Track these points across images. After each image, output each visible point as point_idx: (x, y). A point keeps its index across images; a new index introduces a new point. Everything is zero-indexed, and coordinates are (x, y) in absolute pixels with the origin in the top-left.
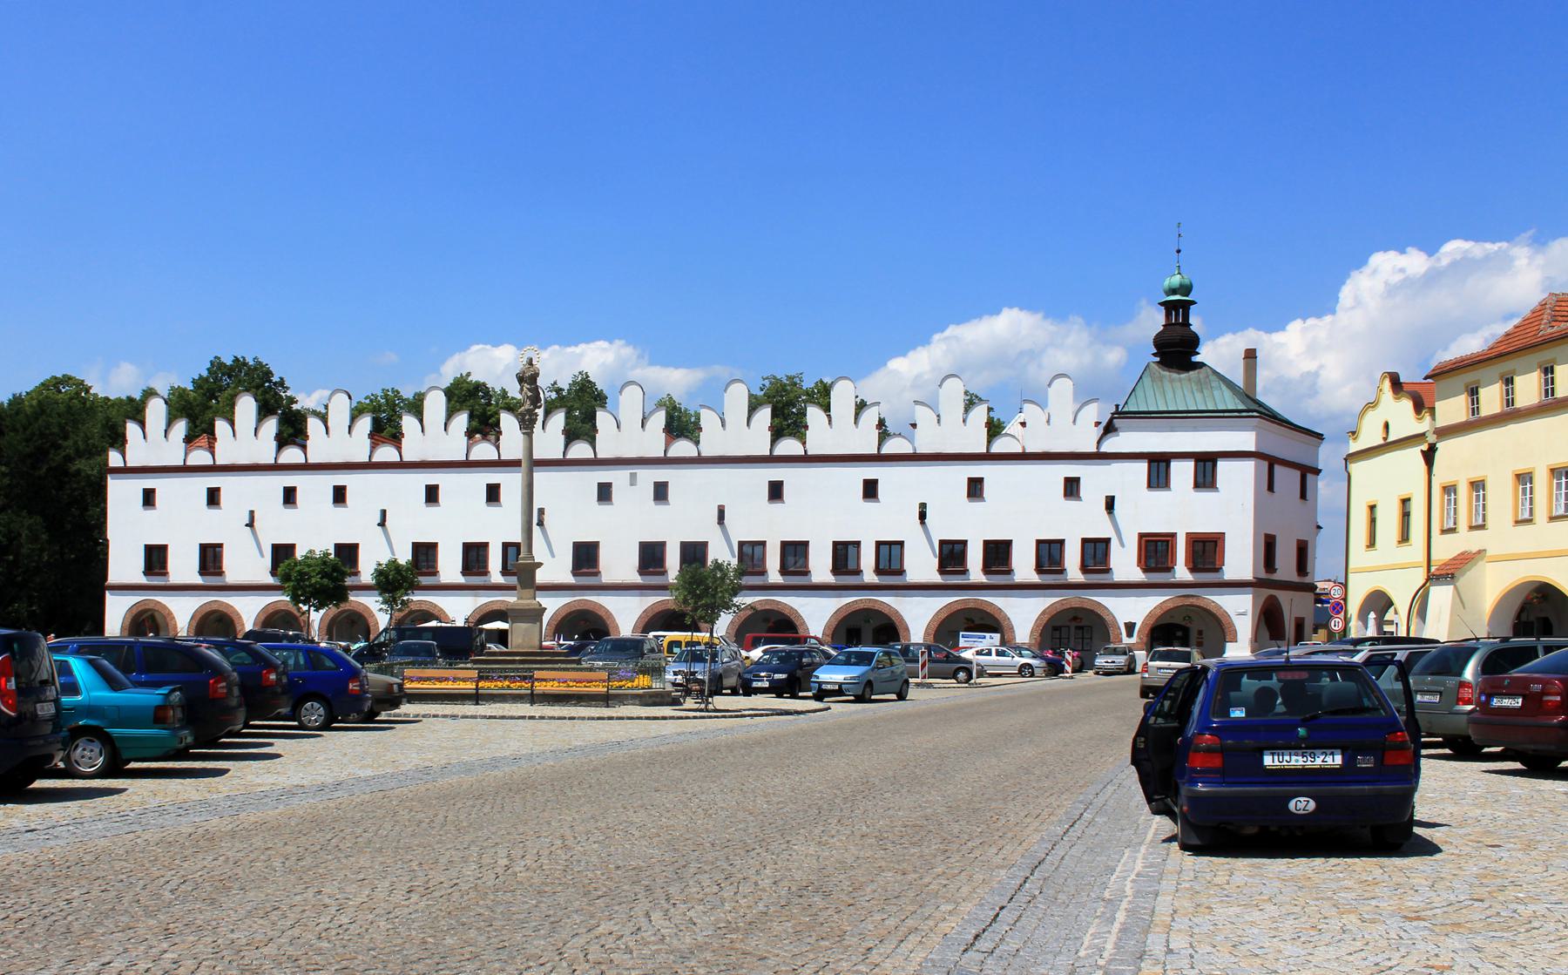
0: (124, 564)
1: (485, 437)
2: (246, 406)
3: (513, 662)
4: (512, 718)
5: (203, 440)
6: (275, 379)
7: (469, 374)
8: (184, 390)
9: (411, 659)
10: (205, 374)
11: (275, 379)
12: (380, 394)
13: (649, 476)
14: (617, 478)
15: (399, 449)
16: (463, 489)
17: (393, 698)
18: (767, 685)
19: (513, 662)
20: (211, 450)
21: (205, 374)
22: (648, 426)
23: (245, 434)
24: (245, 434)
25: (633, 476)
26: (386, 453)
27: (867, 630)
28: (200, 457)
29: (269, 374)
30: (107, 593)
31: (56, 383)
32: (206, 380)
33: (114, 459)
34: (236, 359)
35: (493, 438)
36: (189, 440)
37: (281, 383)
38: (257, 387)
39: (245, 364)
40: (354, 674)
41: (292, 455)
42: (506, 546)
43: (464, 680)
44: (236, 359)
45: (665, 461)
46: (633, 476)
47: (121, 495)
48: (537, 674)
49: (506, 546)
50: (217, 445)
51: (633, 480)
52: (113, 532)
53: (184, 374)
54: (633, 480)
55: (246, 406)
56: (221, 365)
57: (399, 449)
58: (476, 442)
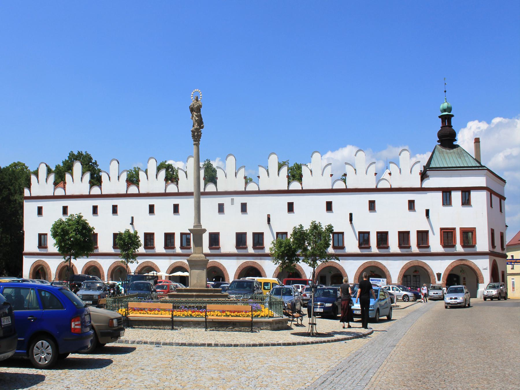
0: (30, 244)
1: (172, 182)
2: (77, 167)
3: (192, 296)
4: (196, 345)
5: (62, 184)
6: (93, 161)
7: (166, 162)
8: (59, 165)
9: (137, 292)
10: (67, 159)
11: (93, 161)
12: (133, 169)
13: (240, 200)
14: (226, 200)
15: (138, 187)
16: (164, 206)
17: (114, 330)
18: (322, 310)
19: (192, 296)
20: (64, 188)
21: (67, 159)
22: (238, 176)
23: (78, 182)
24: (78, 182)
25: (232, 200)
26: (133, 189)
27: (460, 278)
28: (60, 192)
29: (91, 159)
30: (24, 257)
31: (15, 165)
32: (68, 161)
33: (27, 193)
34: (79, 153)
35: (175, 183)
36: (56, 184)
37: (95, 163)
38: (86, 165)
39: (82, 155)
40: (78, 312)
41: (96, 191)
42: (182, 234)
43: (165, 310)
44: (79, 153)
45: (245, 193)
46: (232, 200)
47: (29, 209)
48: (209, 307)
49: (182, 234)
50: (67, 186)
51: (232, 203)
52: (26, 228)
53: (58, 160)
54: (232, 203)
55: (77, 167)
56: (73, 155)
57: (138, 187)
58: (169, 184)
